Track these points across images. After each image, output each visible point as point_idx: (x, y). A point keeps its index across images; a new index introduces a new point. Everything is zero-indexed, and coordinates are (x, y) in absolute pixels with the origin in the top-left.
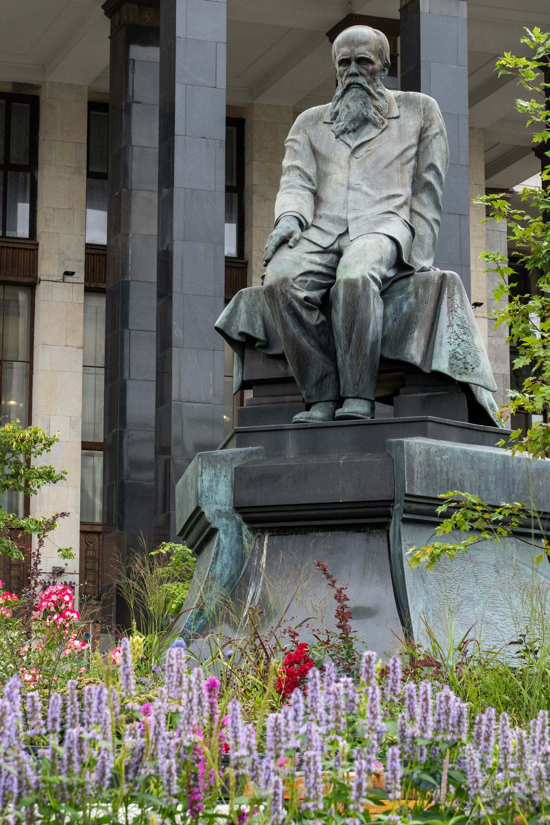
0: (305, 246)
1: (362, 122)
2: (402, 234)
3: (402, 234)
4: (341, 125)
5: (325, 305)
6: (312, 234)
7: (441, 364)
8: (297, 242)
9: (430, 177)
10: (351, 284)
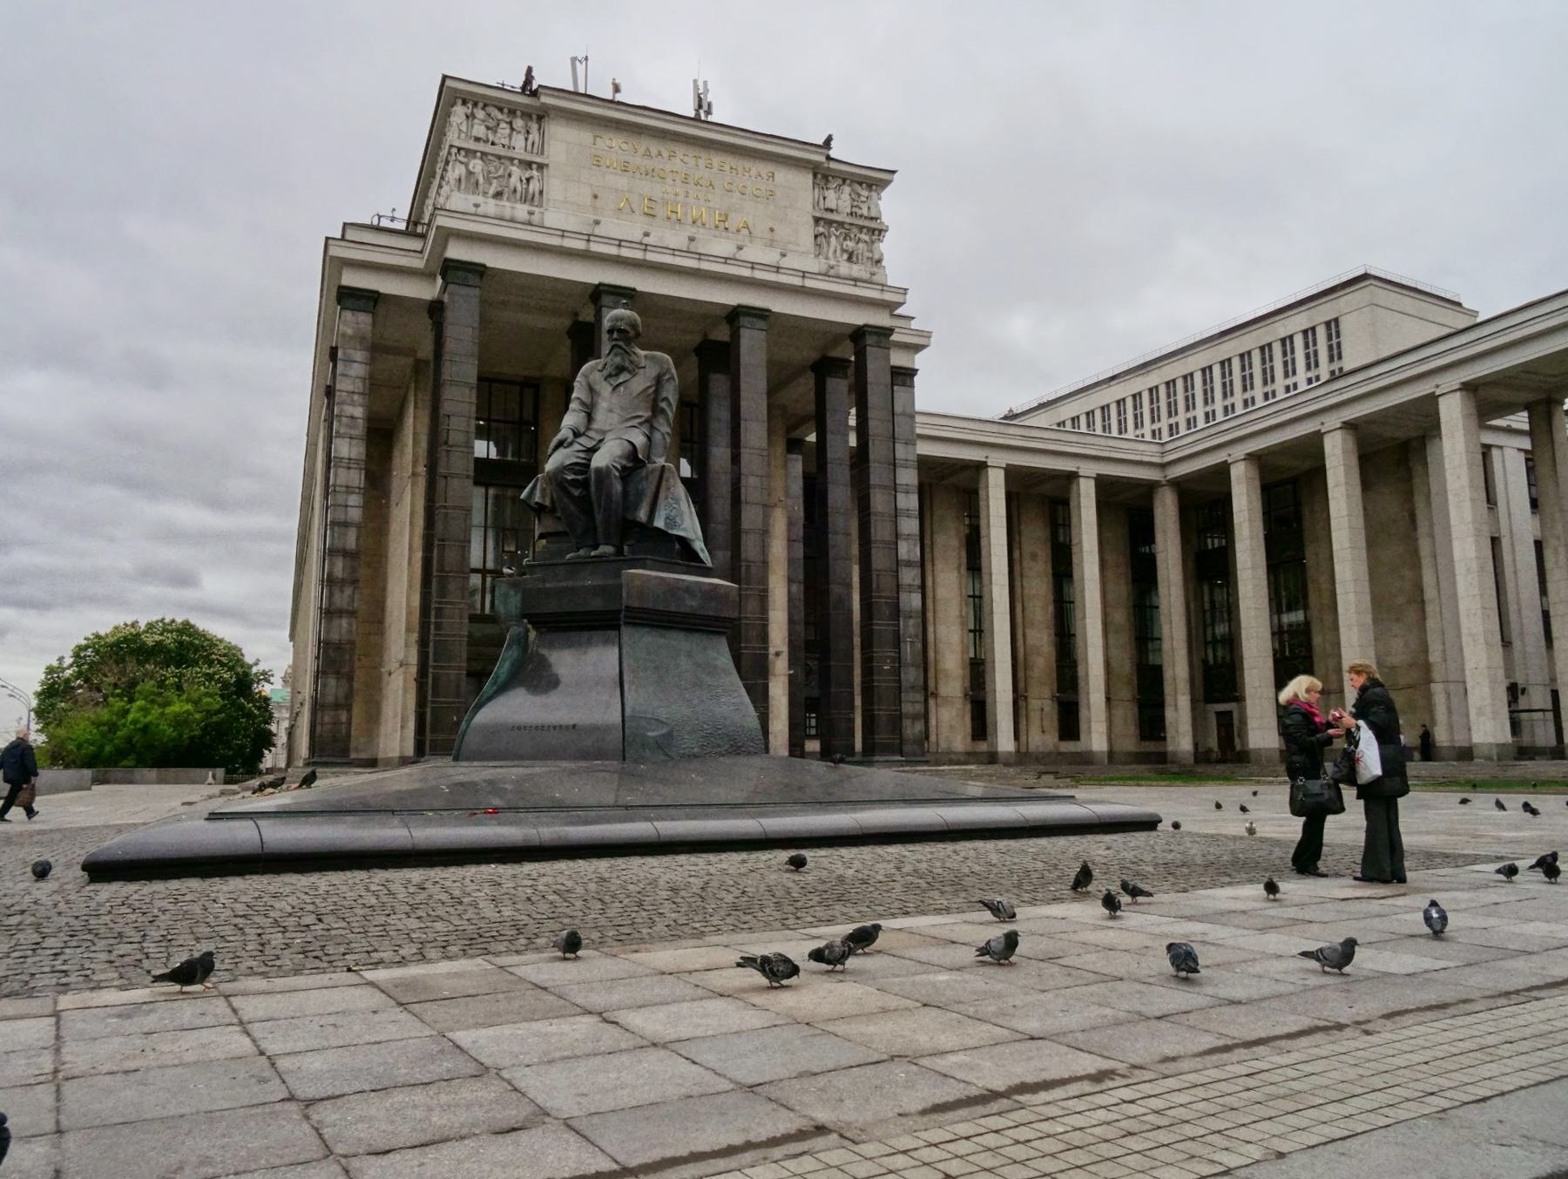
0: (577, 447)
1: (620, 369)
2: (639, 439)
3: (639, 439)
4: (605, 373)
5: (585, 484)
6: (582, 440)
7: (659, 523)
8: (571, 444)
9: (663, 405)
10: (598, 471)
